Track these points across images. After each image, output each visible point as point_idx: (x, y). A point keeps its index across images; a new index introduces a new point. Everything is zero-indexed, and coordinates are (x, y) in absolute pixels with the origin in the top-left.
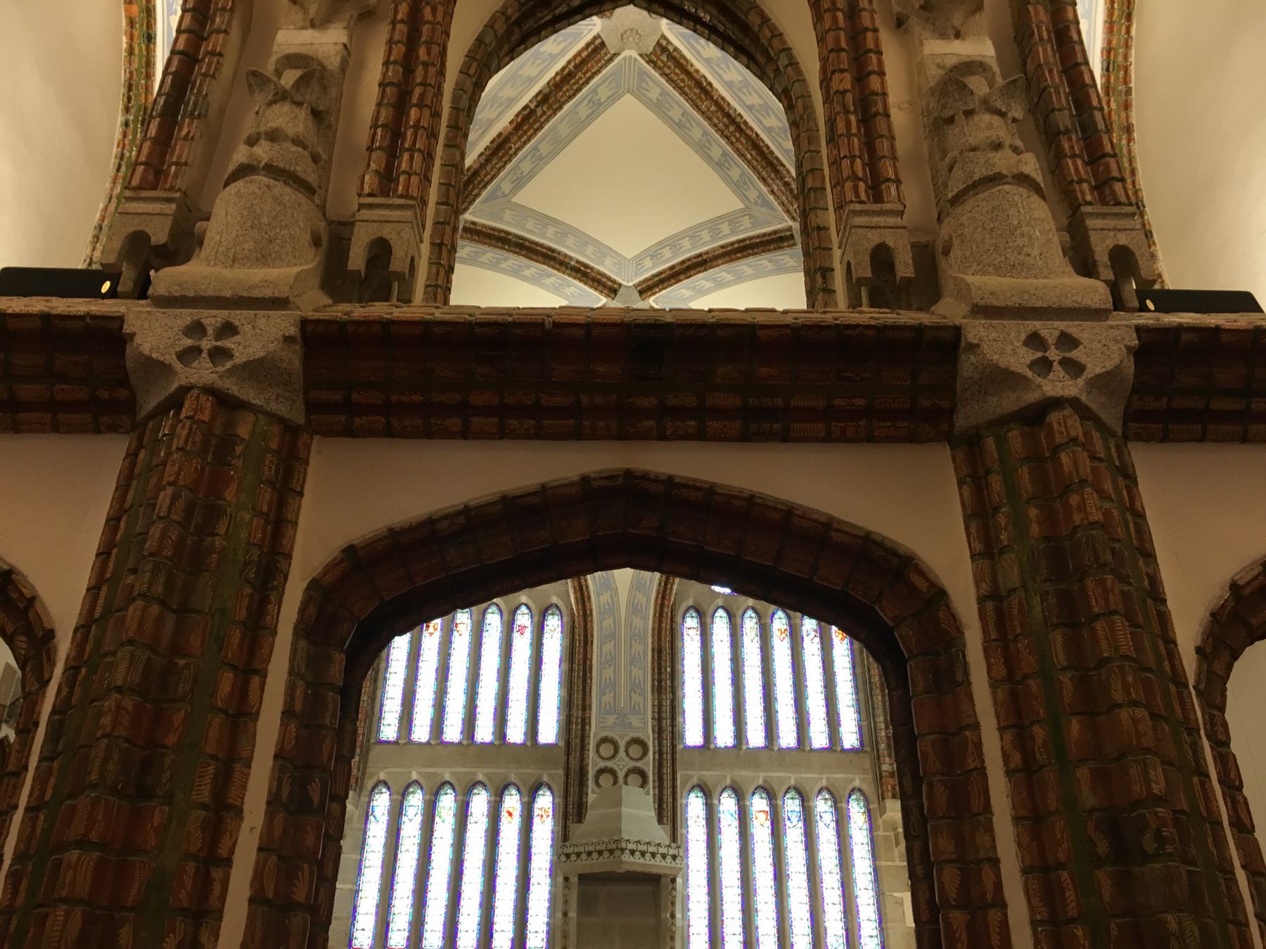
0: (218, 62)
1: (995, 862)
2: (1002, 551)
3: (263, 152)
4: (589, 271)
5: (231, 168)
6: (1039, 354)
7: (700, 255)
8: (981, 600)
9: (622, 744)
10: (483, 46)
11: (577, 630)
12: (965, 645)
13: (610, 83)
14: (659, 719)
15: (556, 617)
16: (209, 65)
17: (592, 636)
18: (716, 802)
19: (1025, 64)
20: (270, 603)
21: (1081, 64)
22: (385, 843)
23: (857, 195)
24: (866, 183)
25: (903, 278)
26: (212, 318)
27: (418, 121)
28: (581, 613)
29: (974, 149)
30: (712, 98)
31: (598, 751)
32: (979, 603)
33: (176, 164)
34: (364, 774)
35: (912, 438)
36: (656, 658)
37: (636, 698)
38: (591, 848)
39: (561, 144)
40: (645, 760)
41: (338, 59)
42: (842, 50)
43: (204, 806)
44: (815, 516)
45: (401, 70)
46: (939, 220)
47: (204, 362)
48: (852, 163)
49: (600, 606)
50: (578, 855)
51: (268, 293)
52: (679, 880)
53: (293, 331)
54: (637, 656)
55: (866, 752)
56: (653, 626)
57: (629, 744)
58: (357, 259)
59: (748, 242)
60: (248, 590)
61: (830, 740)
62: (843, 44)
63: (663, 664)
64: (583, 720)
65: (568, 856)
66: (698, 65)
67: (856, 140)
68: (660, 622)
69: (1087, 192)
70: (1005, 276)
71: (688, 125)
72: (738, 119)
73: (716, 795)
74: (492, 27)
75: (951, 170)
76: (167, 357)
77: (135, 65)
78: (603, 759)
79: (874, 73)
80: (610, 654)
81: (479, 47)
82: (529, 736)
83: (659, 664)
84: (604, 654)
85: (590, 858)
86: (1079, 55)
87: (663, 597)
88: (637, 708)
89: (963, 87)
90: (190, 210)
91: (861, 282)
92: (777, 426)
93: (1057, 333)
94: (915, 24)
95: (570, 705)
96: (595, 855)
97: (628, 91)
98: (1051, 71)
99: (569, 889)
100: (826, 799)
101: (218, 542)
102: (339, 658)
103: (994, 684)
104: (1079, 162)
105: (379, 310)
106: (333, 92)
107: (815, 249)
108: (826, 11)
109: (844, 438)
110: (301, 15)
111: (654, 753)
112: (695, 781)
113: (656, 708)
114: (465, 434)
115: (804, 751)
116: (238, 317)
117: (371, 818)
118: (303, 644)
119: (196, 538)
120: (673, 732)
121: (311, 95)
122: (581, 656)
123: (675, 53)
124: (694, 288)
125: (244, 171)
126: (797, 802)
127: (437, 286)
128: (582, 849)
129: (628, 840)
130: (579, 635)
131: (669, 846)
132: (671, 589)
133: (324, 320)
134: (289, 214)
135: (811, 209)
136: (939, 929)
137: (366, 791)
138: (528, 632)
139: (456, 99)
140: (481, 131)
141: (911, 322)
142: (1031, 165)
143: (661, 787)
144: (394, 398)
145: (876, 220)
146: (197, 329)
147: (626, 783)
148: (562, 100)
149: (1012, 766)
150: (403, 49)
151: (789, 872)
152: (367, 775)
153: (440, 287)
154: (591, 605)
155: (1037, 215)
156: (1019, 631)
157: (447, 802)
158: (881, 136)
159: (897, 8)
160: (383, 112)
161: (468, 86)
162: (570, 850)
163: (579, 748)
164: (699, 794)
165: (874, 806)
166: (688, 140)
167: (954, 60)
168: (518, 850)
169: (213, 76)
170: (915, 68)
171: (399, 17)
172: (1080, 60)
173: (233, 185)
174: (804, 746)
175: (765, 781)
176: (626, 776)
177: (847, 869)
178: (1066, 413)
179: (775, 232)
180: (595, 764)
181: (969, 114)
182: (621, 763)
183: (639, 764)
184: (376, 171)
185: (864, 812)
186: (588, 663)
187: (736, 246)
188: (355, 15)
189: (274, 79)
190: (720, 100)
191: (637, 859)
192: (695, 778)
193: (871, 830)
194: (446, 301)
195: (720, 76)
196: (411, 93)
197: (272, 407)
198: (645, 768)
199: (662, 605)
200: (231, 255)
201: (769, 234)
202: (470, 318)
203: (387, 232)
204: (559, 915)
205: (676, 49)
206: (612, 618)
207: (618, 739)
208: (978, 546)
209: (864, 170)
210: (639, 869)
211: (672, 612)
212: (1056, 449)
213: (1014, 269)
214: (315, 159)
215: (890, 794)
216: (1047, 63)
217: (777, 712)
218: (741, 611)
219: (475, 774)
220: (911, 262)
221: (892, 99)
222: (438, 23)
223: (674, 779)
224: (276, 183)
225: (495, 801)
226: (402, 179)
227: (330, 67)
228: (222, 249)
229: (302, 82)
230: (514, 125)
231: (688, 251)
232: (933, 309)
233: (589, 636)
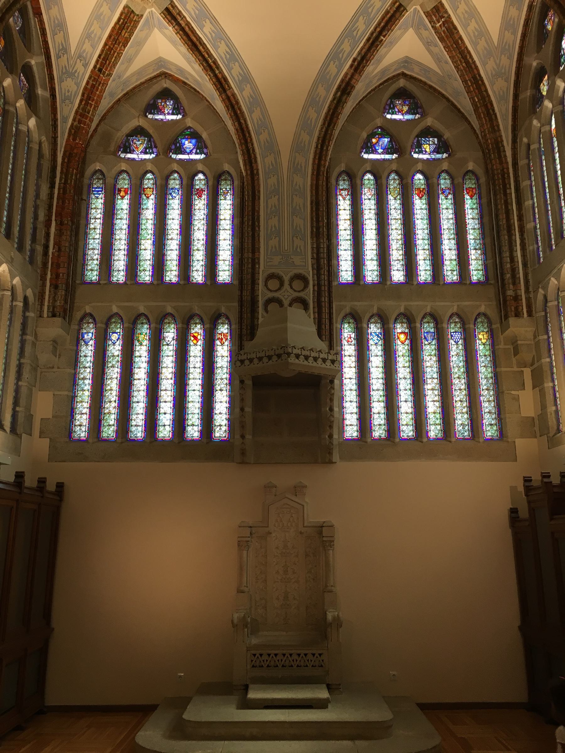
9: (286, 279)
14: (317, 259)
17: (259, 192)
18: (365, 326)
28: (249, 172)
31: (266, 285)
34: (72, 308)
36: (314, 209)
38: (262, 354)
40: (308, 290)
52: (336, 382)
54: (298, 208)
55: (491, 284)
56: (312, 183)
57: (292, 280)
64: (253, 260)
65: (242, 362)
68: (318, 180)
73: (365, 320)
78: (271, 291)
80: (275, 206)
83: (317, 215)
85: (261, 362)
87: (320, 159)
88: (299, 250)
95: (242, 251)
96: (265, 360)
99: (244, 389)
100: (456, 322)
112: (348, 310)
113: (315, 251)
115: (440, 285)
120: (329, 271)
122: (250, 209)
128: (253, 356)
129: (294, 347)
130: (248, 192)
131: (329, 353)
132: (327, 150)
143: (320, 313)
154: (257, 166)
164: (351, 321)
165: (496, 326)
168: (203, 365)
174: (439, 281)
175: (406, 309)
177: (473, 374)
183: (302, 294)
185: (488, 331)
186: (256, 214)
191: (302, 360)
192: (348, 308)
198: (306, 297)
199: (319, 165)
204: (237, 410)
207: (281, 274)
211: (327, 174)
215: (513, 314)
218: (386, 174)
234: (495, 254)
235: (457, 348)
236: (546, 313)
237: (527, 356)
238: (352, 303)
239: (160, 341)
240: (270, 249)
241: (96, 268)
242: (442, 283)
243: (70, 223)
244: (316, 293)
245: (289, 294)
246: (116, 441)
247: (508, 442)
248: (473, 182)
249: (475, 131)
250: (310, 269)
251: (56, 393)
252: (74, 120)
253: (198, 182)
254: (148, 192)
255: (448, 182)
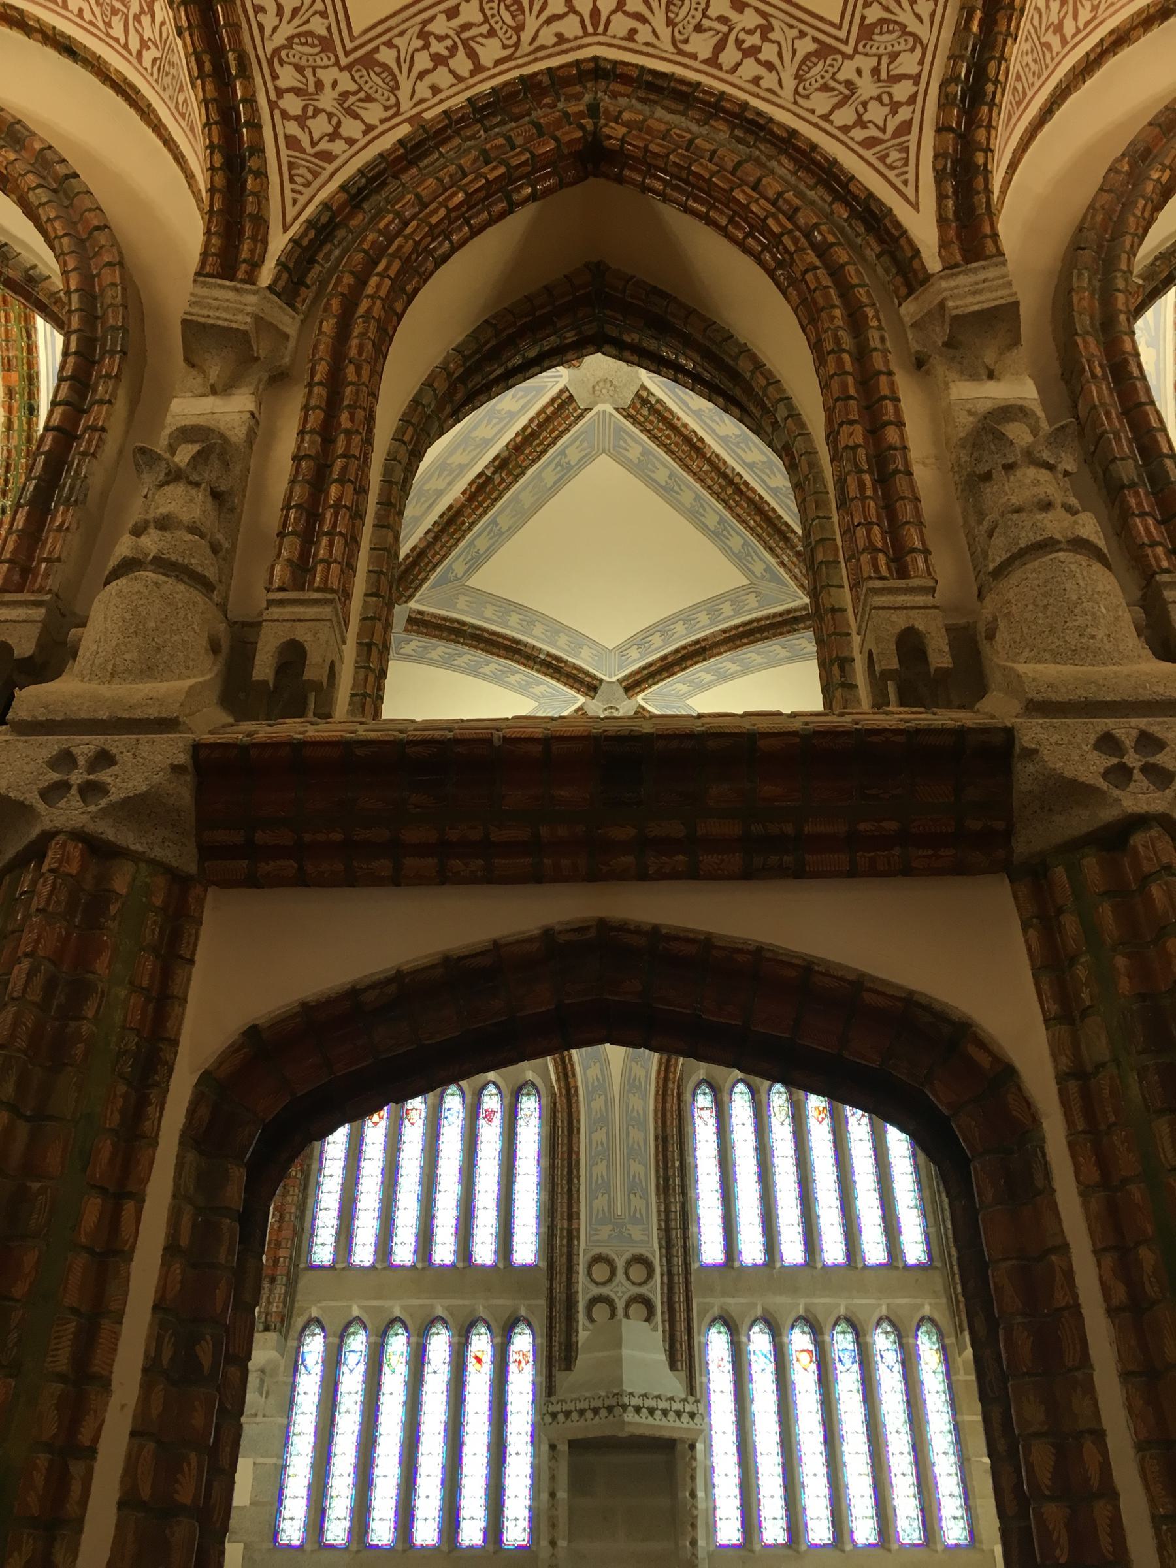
0: (100, 438)
1: (1099, 1435)
2: (1085, 1013)
3: (152, 543)
4: (562, 665)
5: (113, 563)
6: (1115, 761)
7: (697, 642)
8: (1061, 1079)
9: (620, 1264)
10: (420, 407)
11: (559, 1115)
12: (1043, 1140)
13: (581, 442)
14: (666, 1231)
15: (533, 1098)
16: (90, 441)
17: (578, 1121)
19: (1076, 407)
20: (151, 1104)
21: (1145, 404)
22: (319, 1402)
23: (876, 568)
24: (886, 554)
25: (937, 669)
26: (84, 746)
27: (340, 499)
28: (564, 1091)
29: (1018, 510)
30: (704, 456)
31: (589, 1274)
32: (1058, 1083)
33: (48, 560)
34: (291, 1309)
35: (960, 870)
37: (636, 1202)
39: (524, 516)
40: (652, 1284)
41: (244, 430)
42: (851, 398)
43: (61, 1377)
44: (840, 974)
45: (318, 439)
46: (980, 596)
47: (74, 799)
48: (869, 532)
49: (587, 1082)
50: (568, 1414)
51: (153, 712)
52: (700, 1446)
53: (182, 758)
54: (636, 1146)
55: (936, 1268)
57: (629, 1263)
58: (264, 668)
59: (755, 624)
60: (122, 1088)
61: (889, 1253)
62: (852, 392)
63: (669, 1154)
64: (570, 1231)
65: (554, 1415)
66: (685, 418)
67: (872, 504)
68: (664, 1101)
69: (1162, 556)
70: (1065, 664)
71: (676, 488)
72: (737, 480)
74: (430, 385)
75: (990, 535)
76: (27, 796)
77: (14, 442)
78: (597, 1283)
79: (891, 423)
81: (415, 410)
82: (501, 1255)
86: (1142, 393)
89: (1001, 437)
90: (63, 616)
91: (886, 675)
92: (788, 859)
93: (1135, 733)
94: (939, 367)
96: (589, 1415)
97: (603, 452)
98: (1108, 414)
101: (86, 1028)
102: (238, 1174)
103: (1085, 1192)
104: (1150, 521)
105: (291, 729)
106: (237, 468)
107: (829, 636)
108: (829, 353)
109: (873, 872)
110: (199, 380)
111: (662, 1275)
112: (716, 1311)
113: (663, 1217)
114: (396, 880)
116: (115, 743)
117: (302, 1368)
118: (191, 1156)
119: (57, 1023)
120: (685, 1246)
121: (210, 474)
122: (565, 1149)
123: (658, 406)
124: (692, 681)
125: (128, 566)
126: (850, 1337)
127: (365, 695)
129: (631, 1394)
131: (685, 1400)
133: (221, 744)
134: (181, 615)
135: (822, 587)
136: (1029, 1527)
137: (294, 1333)
138: (497, 1120)
139: (387, 471)
140: (427, 505)
141: (950, 724)
142: (1089, 527)
144: (307, 838)
145: (902, 599)
146: (65, 760)
147: (627, 1316)
148: (524, 464)
149: (1115, 1302)
150: (322, 416)
151: (843, 1433)
152: (295, 1311)
153: (369, 696)
154: (576, 1082)
155: (1100, 588)
156: (1112, 1119)
157: (398, 1346)
158: (902, 498)
159: (915, 347)
160: (297, 490)
161: (403, 455)
162: (557, 1408)
163: (565, 1271)
164: (722, 1329)
166: (677, 506)
167: (990, 405)
168: (490, 1409)
169: (94, 455)
170: (940, 416)
171: (317, 378)
172: (1144, 399)
173: (114, 583)
174: (855, 1262)
175: (807, 1310)
176: (627, 1306)
177: (919, 1427)
178: (1153, 833)
179: (789, 612)
180: (585, 1287)
181: (1009, 468)
182: (620, 1289)
183: (643, 1290)
184: (289, 560)
185: (938, 1350)
187: (741, 629)
188: (265, 376)
189: (167, 456)
190: (714, 458)
191: (644, 1419)
193: (948, 1374)
194: (377, 713)
195: (714, 431)
196: (331, 466)
197: (158, 853)
198: (651, 1296)
199: (666, 1080)
200: (110, 668)
201: (781, 614)
202: (401, 736)
203: (302, 633)
204: (545, 1496)
205: (659, 401)
206: (603, 1097)
207: (613, 1256)
208: (1054, 1008)
209: (884, 539)
210: (648, 1433)
212: (1145, 880)
213: (1075, 655)
214: (215, 549)
216: (1103, 404)
217: (819, 1217)
219: (432, 1307)
220: (947, 649)
221: (914, 454)
222: (363, 383)
223: (689, 1309)
224: (166, 579)
225: (459, 1343)
226: (319, 568)
227: (233, 439)
228: (97, 662)
229: (200, 458)
230: (467, 496)
231: (682, 638)
232: (978, 706)
238: (722, 1300)
239: (423, 1364)
240: (595, 1212)
241: (331, 1240)
242: (860, 1265)
243: (299, 1176)
244: (666, 1288)
246: (347, 1548)
251: (260, 1460)
253: (486, 1099)
254: (413, 1114)
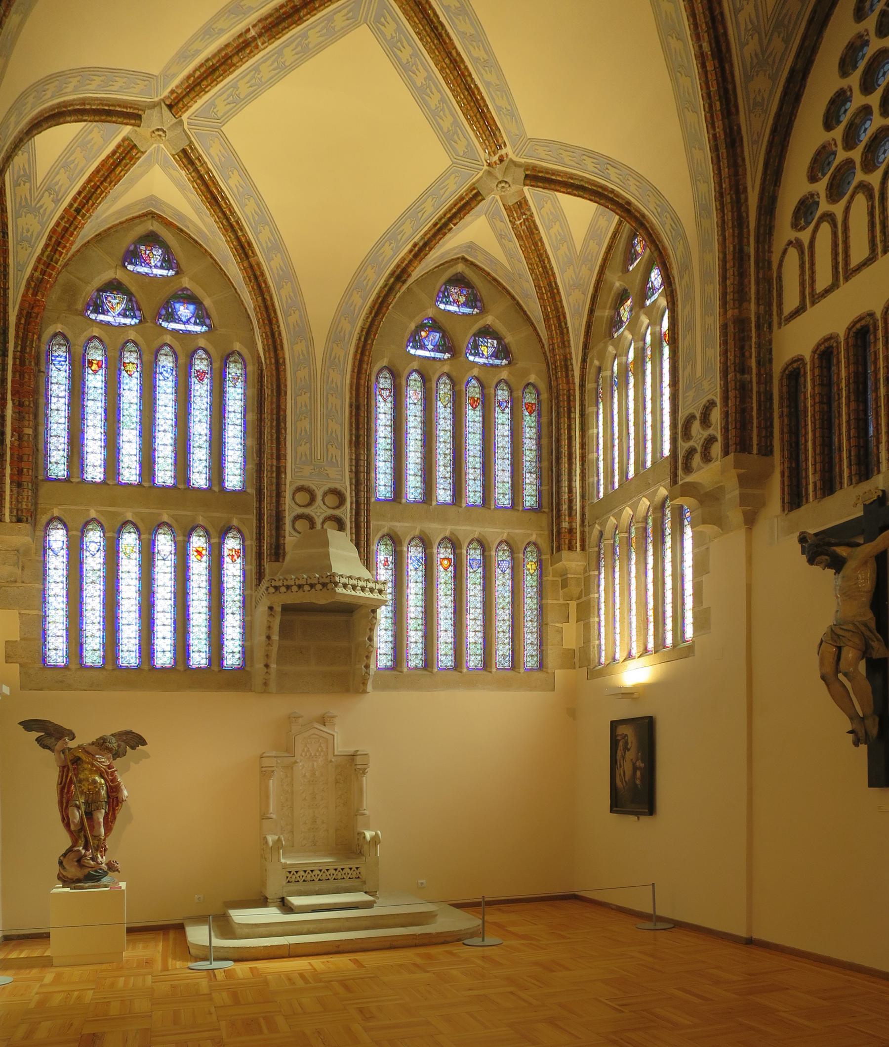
18: (405, 549)
84: (299, 405)
88: (334, 460)
100: (504, 550)
193: (540, 576)
215: (566, 547)
233: (282, 385)
234: (552, 481)
235: (504, 577)
236: (600, 549)
237: (574, 589)
245: (321, 510)
247: (547, 672)
248: (534, 397)
249: (541, 340)
250: (348, 483)
252: (35, 269)
255: (506, 393)
